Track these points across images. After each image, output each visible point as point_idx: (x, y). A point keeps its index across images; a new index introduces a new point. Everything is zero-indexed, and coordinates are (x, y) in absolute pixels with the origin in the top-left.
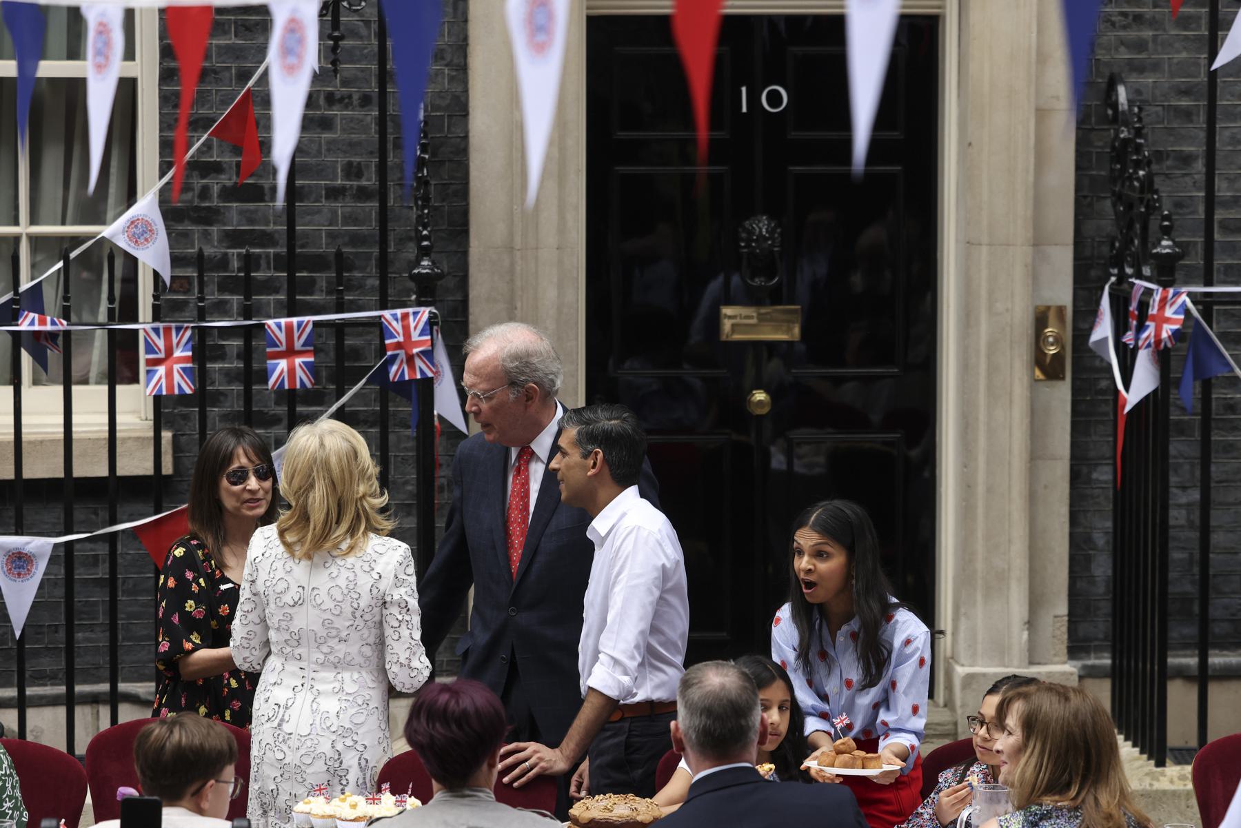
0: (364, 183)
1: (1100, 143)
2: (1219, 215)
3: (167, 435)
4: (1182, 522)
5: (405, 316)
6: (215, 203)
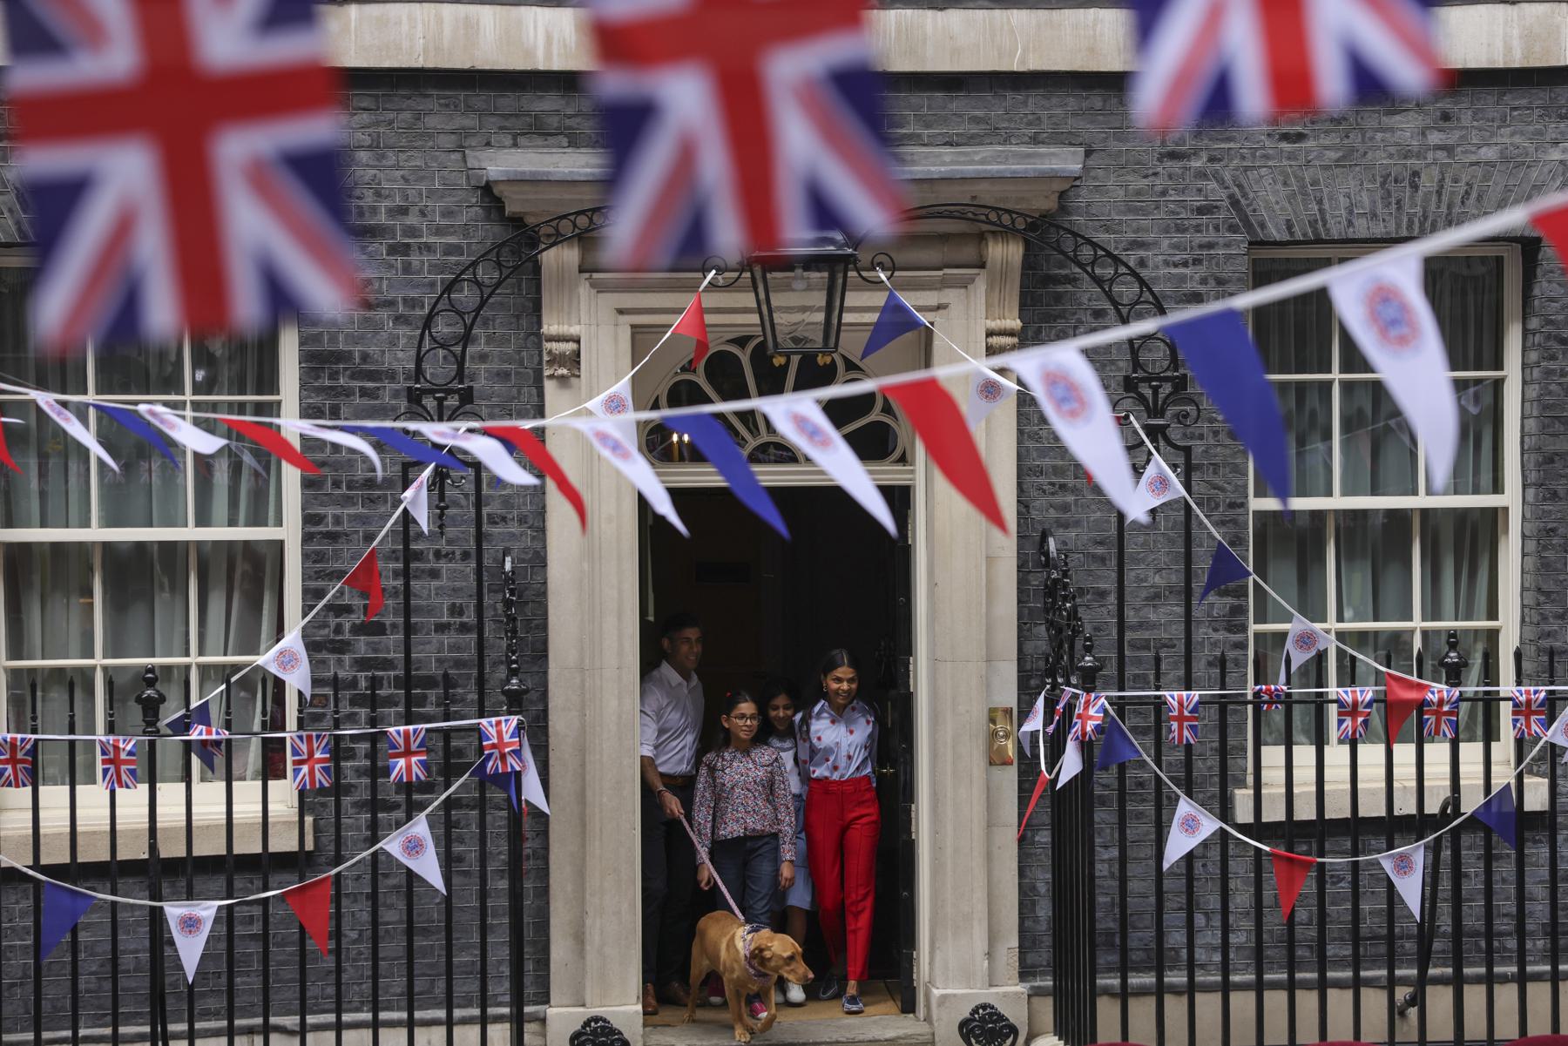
0: (465, 619)
1: (1036, 581)
2: (1129, 636)
3: (309, 819)
4: (1106, 873)
5: (499, 723)
6: (347, 636)
